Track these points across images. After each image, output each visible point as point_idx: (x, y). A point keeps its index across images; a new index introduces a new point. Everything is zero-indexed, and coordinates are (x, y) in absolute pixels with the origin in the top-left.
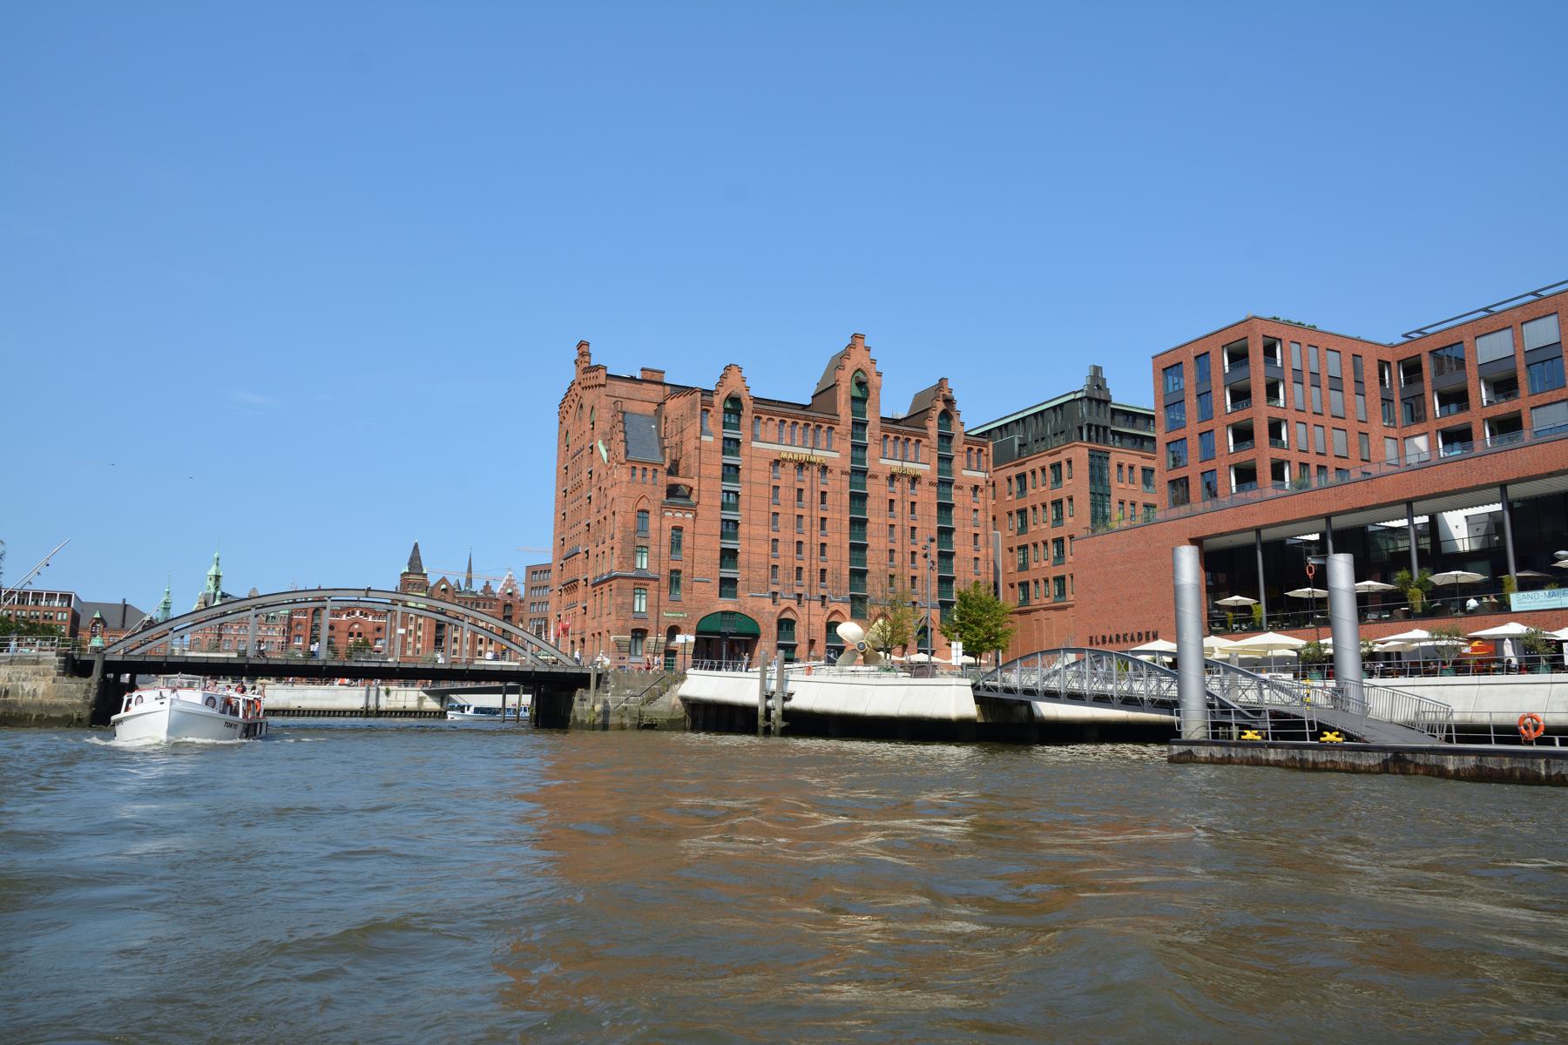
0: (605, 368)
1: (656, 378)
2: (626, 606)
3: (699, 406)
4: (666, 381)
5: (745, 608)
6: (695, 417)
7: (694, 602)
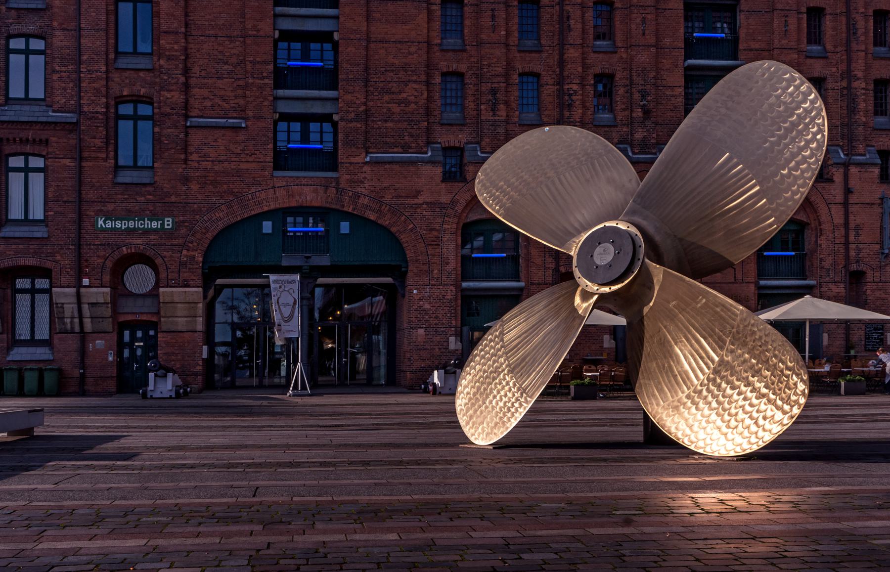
5: (357, 196)
7: (194, 187)
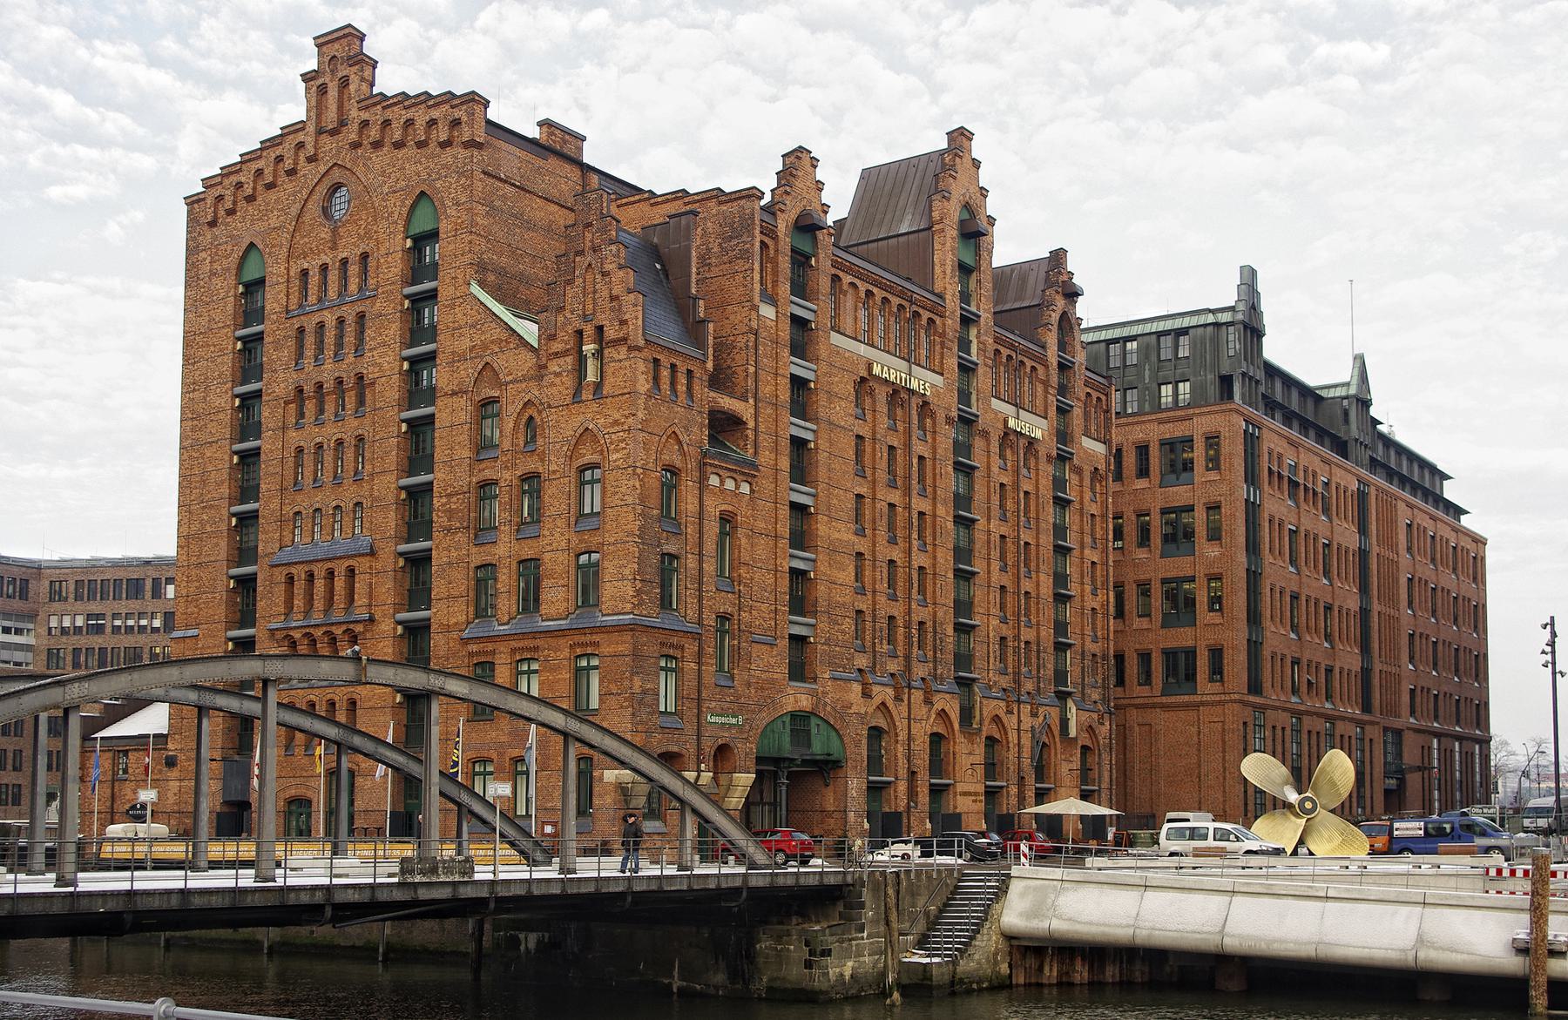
0: (486, 104)
1: (569, 150)
2: (648, 699)
3: (757, 232)
4: (588, 159)
6: (746, 255)
